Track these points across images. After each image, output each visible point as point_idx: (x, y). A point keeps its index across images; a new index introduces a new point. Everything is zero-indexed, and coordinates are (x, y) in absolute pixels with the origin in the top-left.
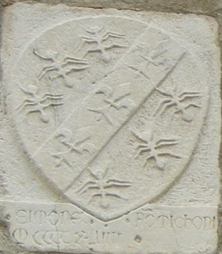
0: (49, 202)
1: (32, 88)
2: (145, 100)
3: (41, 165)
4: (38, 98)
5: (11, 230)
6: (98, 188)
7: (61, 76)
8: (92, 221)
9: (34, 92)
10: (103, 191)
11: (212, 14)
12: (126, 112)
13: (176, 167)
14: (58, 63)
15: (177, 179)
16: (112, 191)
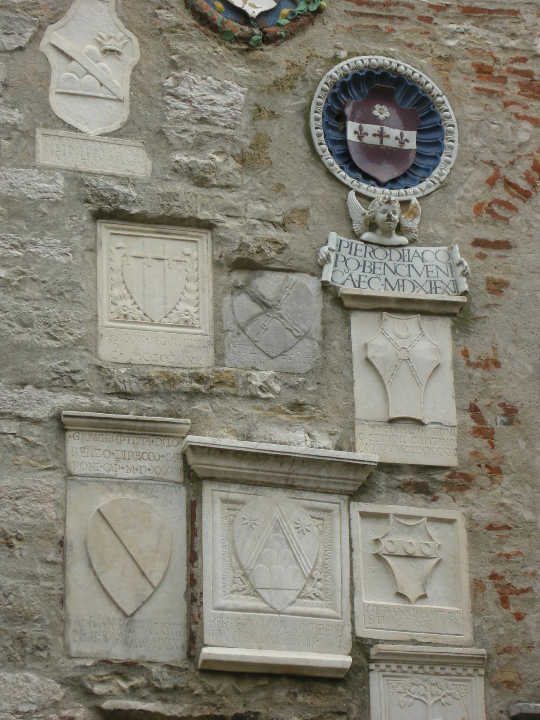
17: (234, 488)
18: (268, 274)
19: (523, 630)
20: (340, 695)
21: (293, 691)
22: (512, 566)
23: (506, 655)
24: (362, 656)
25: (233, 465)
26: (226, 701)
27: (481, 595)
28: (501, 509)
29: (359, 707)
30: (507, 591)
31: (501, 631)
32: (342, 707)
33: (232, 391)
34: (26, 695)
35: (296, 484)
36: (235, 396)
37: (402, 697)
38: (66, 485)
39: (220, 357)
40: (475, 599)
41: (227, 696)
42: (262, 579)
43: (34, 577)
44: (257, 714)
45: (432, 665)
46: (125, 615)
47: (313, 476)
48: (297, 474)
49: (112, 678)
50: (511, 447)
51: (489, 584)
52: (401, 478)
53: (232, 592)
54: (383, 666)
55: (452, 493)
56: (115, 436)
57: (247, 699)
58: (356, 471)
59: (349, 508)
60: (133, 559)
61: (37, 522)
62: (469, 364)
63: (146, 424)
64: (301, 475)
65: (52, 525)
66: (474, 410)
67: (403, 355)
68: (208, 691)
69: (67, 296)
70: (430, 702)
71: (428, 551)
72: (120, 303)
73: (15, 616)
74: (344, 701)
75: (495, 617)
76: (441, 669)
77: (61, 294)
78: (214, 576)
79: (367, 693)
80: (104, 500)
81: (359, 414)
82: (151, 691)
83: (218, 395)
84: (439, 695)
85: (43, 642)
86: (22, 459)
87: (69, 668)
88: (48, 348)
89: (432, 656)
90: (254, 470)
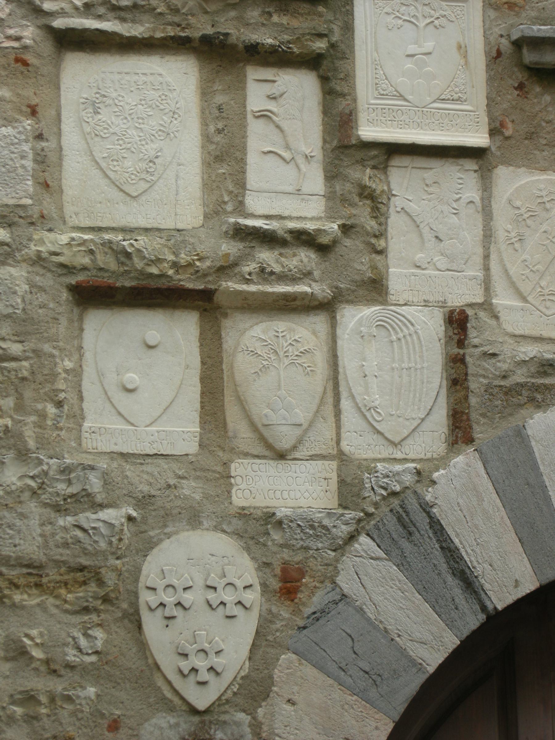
0: (519, 304)
3: (515, 280)
4: (513, 234)
5: (501, 320)
6: (544, 295)
7: (524, 220)
8: (541, 317)
9: (510, 230)
10: (547, 297)
14: (523, 210)
20: (320, 15)
21: (267, 10)
26: (192, 20)
29: (342, 28)
32: (322, 29)
37: (389, 19)
41: (193, 15)
44: (227, 35)
57: (216, 19)
68: (171, 10)
70: (422, 24)
74: (326, 22)
79: (350, 13)
82: (108, 9)
84: (432, 17)
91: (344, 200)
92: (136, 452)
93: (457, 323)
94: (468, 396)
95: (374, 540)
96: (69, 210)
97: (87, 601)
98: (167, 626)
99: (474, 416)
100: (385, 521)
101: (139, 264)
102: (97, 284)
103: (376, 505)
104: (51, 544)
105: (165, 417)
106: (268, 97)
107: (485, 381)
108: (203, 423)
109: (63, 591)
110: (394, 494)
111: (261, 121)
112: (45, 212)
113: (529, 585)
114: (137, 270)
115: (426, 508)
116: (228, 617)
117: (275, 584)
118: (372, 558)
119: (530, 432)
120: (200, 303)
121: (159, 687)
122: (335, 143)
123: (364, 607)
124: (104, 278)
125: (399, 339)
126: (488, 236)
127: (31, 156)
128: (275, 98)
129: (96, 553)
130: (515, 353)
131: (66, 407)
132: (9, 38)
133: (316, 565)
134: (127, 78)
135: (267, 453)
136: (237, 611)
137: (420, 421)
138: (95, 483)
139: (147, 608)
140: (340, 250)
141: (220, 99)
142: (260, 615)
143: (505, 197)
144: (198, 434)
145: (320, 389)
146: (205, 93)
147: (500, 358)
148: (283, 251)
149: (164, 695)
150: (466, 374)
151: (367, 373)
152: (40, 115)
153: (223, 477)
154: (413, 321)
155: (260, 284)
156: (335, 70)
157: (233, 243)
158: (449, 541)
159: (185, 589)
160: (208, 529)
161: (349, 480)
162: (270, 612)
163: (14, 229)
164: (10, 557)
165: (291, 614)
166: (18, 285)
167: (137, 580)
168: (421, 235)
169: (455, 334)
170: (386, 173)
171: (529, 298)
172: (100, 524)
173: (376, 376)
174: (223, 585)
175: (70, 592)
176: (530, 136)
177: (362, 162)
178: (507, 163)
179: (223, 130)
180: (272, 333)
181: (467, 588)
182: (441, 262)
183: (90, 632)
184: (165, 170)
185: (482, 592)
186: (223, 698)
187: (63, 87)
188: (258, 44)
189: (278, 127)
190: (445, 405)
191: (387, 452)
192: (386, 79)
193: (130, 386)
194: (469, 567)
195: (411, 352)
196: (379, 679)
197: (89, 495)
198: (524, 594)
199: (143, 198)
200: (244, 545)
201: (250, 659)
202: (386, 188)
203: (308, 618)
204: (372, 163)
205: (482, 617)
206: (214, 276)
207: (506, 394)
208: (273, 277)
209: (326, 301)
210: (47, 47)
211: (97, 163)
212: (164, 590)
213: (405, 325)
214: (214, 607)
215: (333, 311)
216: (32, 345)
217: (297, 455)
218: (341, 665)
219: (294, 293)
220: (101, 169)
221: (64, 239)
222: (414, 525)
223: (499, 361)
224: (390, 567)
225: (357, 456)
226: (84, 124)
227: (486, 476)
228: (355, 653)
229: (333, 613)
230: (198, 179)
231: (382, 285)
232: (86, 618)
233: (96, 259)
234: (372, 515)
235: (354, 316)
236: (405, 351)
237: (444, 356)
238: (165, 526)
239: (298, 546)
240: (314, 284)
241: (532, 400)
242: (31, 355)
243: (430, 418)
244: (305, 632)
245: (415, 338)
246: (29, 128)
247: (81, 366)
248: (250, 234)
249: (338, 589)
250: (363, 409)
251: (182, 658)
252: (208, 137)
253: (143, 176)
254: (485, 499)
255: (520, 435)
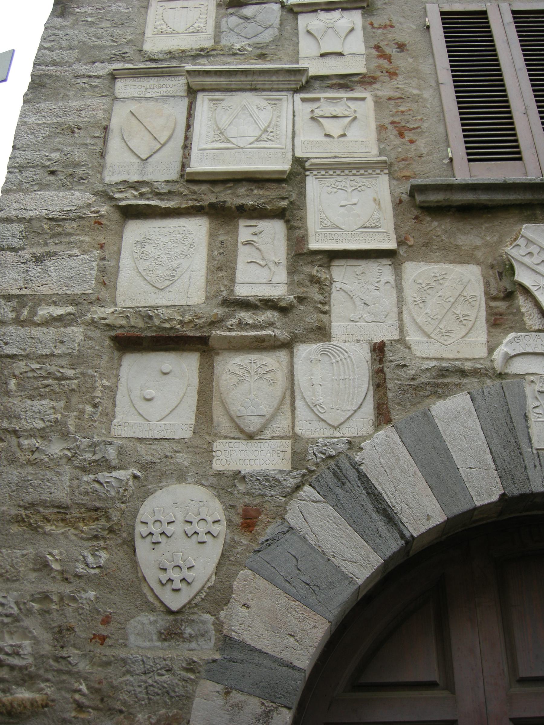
0: (425, 339)
1: (415, 295)
2: (457, 299)
4: (418, 299)
5: (412, 349)
10: (445, 334)
11: (478, 264)
12: (450, 303)
13: (470, 324)
14: (423, 285)
15: (471, 329)
16: (447, 334)
17: (217, 93)
18: (250, 6)
19: (415, 148)
20: (284, 188)
22: (406, 117)
23: (403, 162)
24: (300, 167)
25: (215, 80)
27: (384, 132)
28: (397, 90)
29: (297, 194)
30: (403, 129)
31: (400, 150)
32: (285, 195)
33: (221, 53)
34: (70, 202)
35: (258, 87)
36: (223, 55)
37: (329, 189)
38: (113, 103)
39: (217, 42)
40: (380, 134)
41: (205, 195)
42: (231, 132)
43: (85, 145)
45: (350, 169)
46: (142, 160)
47: (268, 81)
48: (257, 81)
49: (128, 190)
50: (402, 62)
51: (390, 127)
52: (330, 82)
53: (213, 142)
54: (315, 172)
55: (364, 86)
56: (146, 78)
58: (295, 75)
59: (293, 97)
60: (150, 132)
61: (91, 120)
62: (373, 28)
63: (164, 69)
64: (260, 81)
65: (101, 120)
66: (378, 48)
67: (330, 25)
69: (126, 25)
70: (350, 190)
71: (346, 113)
72: (159, 27)
73: (70, 164)
74: (286, 191)
75: (395, 143)
76: (357, 171)
77: (123, 24)
78: (200, 134)
80: (134, 107)
81: (301, 54)
83: (211, 56)
85: (86, 175)
86: (86, 93)
87: (99, 187)
88: (111, 46)
89: (349, 164)
90: (229, 81)
91: (300, 284)
92: (148, 437)
93: (379, 350)
94: (386, 393)
95: (315, 489)
96: (119, 299)
97: (97, 531)
98: (154, 549)
99: (391, 404)
100: (323, 475)
101: (157, 322)
102: (129, 335)
103: (317, 465)
104: (77, 492)
105: (171, 416)
106: (252, 234)
107: (399, 382)
108: (197, 418)
109: (81, 525)
110: (331, 457)
111: (247, 246)
112: (101, 297)
113: (439, 518)
114: (155, 326)
115: (356, 466)
116: (199, 543)
117: (238, 520)
118: (313, 501)
119: (433, 413)
120: (200, 346)
121: (145, 594)
122: (293, 253)
123: (307, 536)
124: (134, 332)
125: (337, 362)
126: (401, 301)
127: (96, 268)
128: (256, 234)
129: (107, 499)
130: (420, 365)
131: (100, 408)
132: (93, 212)
133: (270, 507)
134: (164, 229)
135: (241, 436)
136: (206, 538)
137: (353, 412)
138: (112, 453)
139: (140, 536)
140: (295, 311)
141: (222, 238)
142: (225, 542)
143: (411, 279)
144: (192, 426)
145: (280, 394)
146: (212, 235)
147: (409, 368)
148: (255, 312)
149: (148, 599)
150: (385, 379)
151: (314, 383)
152: (105, 248)
153: (207, 451)
154: (347, 350)
155: (239, 331)
156: (294, 215)
157: (221, 308)
158: (374, 488)
159: (168, 523)
160: (190, 483)
161: (299, 451)
162: (233, 540)
163: (79, 306)
164: (46, 500)
165: (249, 541)
166: (77, 337)
167: (135, 517)
168: (354, 303)
169: (377, 356)
170: (329, 270)
171: (432, 335)
172: (113, 479)
173: (320, 385)
174: (197, 521)
175: (85, 525)
176: (426, 245)
177: (312, 263)
178: (412, 260)
179: (223, 253)
180: (247, 361)
181: (389, 522)
182: (369, 318)
183: (97, 553)
184: (183, 274)
185: (400, 524)
186: (193, 602)
187: (124, 237)
188: (244, 204)
189: (257, 249)
190: (372, 402)
191: (329, 432)
192: (327, 219)
193: (148, 397)
194: (390, 507)
195: (346, 368)
196: (318, 589)
197: (106, 461)
198: (435, 525)
199: (167, 290)
200: (216, 494)
201: (216, 574)
202: (328, 276)
203: (262, 544)
204: (318, 263)
205: (401, 543)
206: (208, 328)
207: (415, 389)
208: (248, 327)
209: (286, 341)
210: (116, 216)
211: (140, 273)
212: (154, 523)
213: (341, 353)
214: (189, 535)
215: (292, 348)
216: (81, 370)
217: (262, 436)
218: (287, 579)
219: (262, 335)
220: (142, 276)
221: (111, 310)
222: (347, 478)
223: (409, 370)
224: (327, 507)
225: (306, 436)
226: (134, 254)
227: (401, 443)
228: (298, 569)
229: (281, 540)
230: (204, 278)
231: (326, 331)
232: (95, 543)
233: (130, 321)
234: (314, 471)
235: (306, 350)
236: (342, 368)
237: (371, 371)
238: (160, 482)
239: (257, 494)
240: (276, 330)
241: (434, 393)
242: (80, 376)
243: (361, 410)
244: (259, 554)
245: (348, 360)
246: (97, 254)
247: (117, 386)
248: (233, 303)
249: (286, 524)
250: (311, 406)
251: (162, 571)
252: (213, 257)
253: (168, 278)
254: (401, 459)
255: (427, 416)
